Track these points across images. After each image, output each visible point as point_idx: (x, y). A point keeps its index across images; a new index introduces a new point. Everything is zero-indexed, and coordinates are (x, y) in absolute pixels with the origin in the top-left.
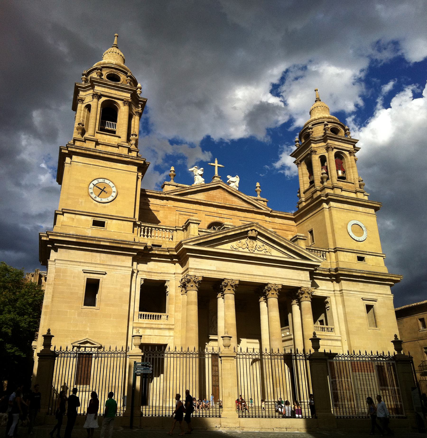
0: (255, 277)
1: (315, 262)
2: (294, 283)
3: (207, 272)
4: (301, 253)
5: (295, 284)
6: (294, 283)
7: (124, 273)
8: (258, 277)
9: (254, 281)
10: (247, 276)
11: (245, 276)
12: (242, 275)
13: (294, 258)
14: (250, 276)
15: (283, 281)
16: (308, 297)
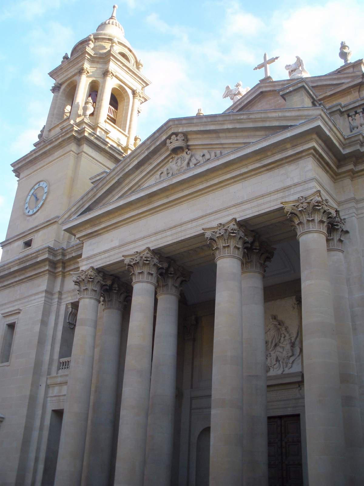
0: (184, 228)
1: (302, 124)
2: (270, 201)
3: (103, 256)
4: (267, 124)
5: (272, 204)
6: (270, 201)
7: (37, 304)
8: (189, 226)
9: (183, 238)
10: (169, 233)
11: (164, 235)
12: (159, 236)
13: (247, 144)
14: (174, 231)
15: (244, 210)
16: (316, 221)
